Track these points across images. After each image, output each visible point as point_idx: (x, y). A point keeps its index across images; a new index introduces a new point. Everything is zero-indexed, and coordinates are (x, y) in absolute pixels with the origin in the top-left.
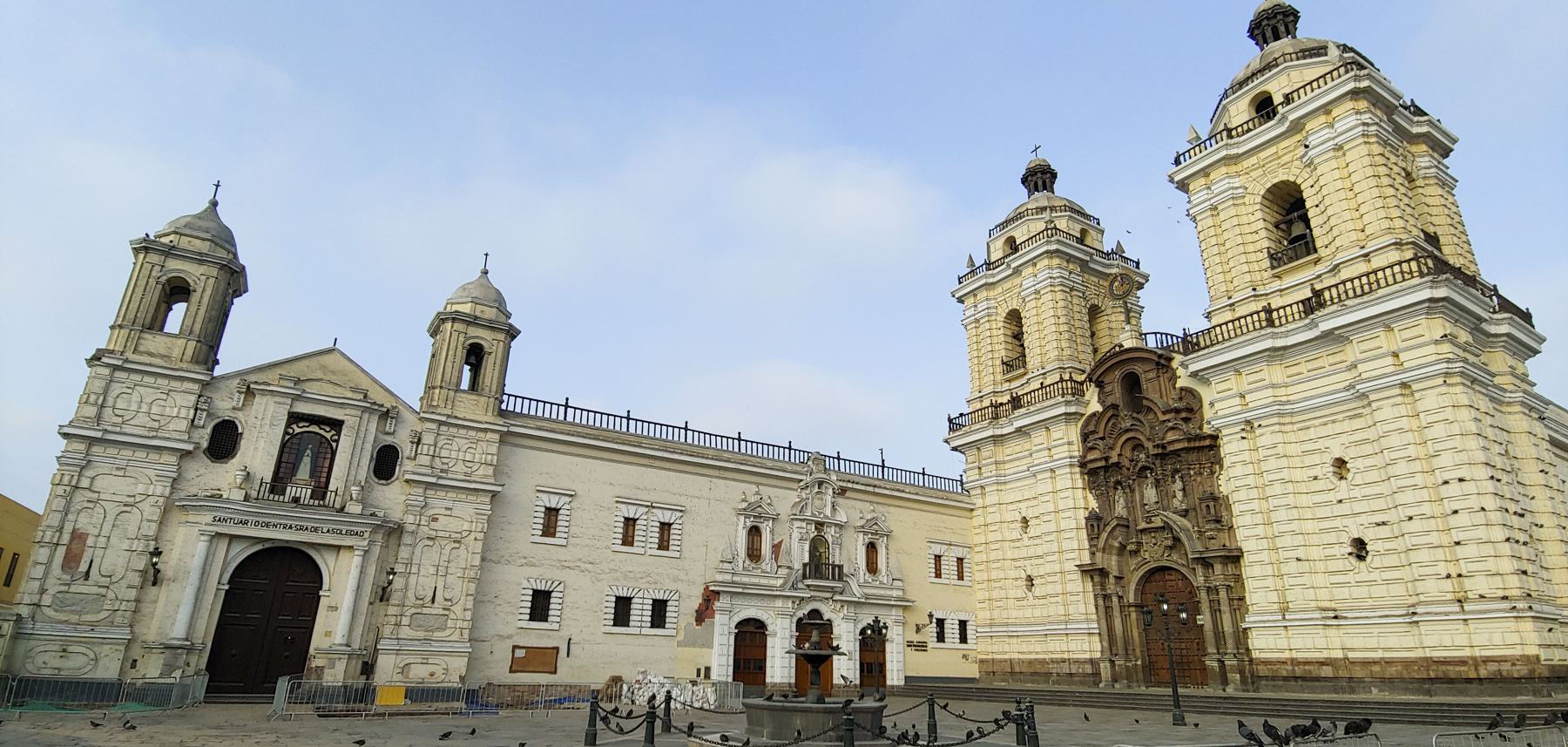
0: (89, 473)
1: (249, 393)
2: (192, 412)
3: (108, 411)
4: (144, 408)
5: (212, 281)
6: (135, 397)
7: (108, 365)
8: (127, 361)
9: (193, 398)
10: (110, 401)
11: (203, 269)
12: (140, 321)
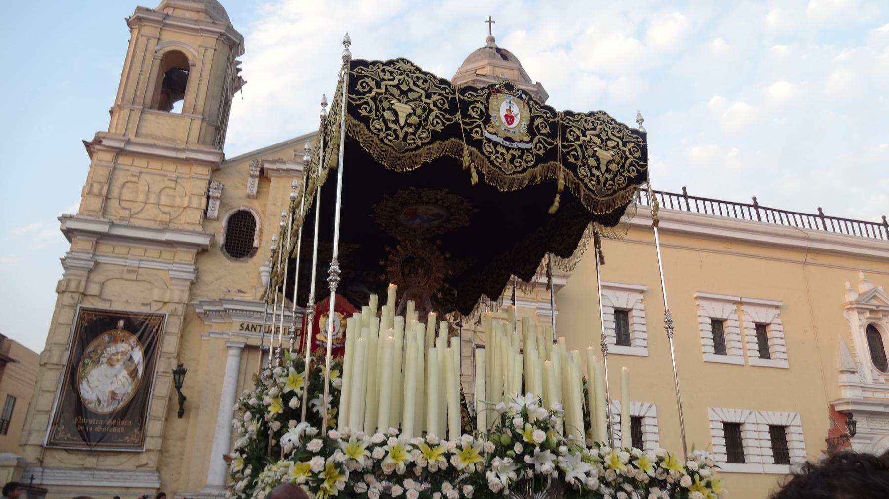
0: (98, 277)
1: (263, 176)
2: (204, 200)
3: (114, 203)
4: (153, 199)
5: (211, 52)
6: (142, 186)
7: (111, 149)
8: (129, 142)
9: (204, 185)
10: (115, 192)
11: (199, 41)
12: (140, 99)
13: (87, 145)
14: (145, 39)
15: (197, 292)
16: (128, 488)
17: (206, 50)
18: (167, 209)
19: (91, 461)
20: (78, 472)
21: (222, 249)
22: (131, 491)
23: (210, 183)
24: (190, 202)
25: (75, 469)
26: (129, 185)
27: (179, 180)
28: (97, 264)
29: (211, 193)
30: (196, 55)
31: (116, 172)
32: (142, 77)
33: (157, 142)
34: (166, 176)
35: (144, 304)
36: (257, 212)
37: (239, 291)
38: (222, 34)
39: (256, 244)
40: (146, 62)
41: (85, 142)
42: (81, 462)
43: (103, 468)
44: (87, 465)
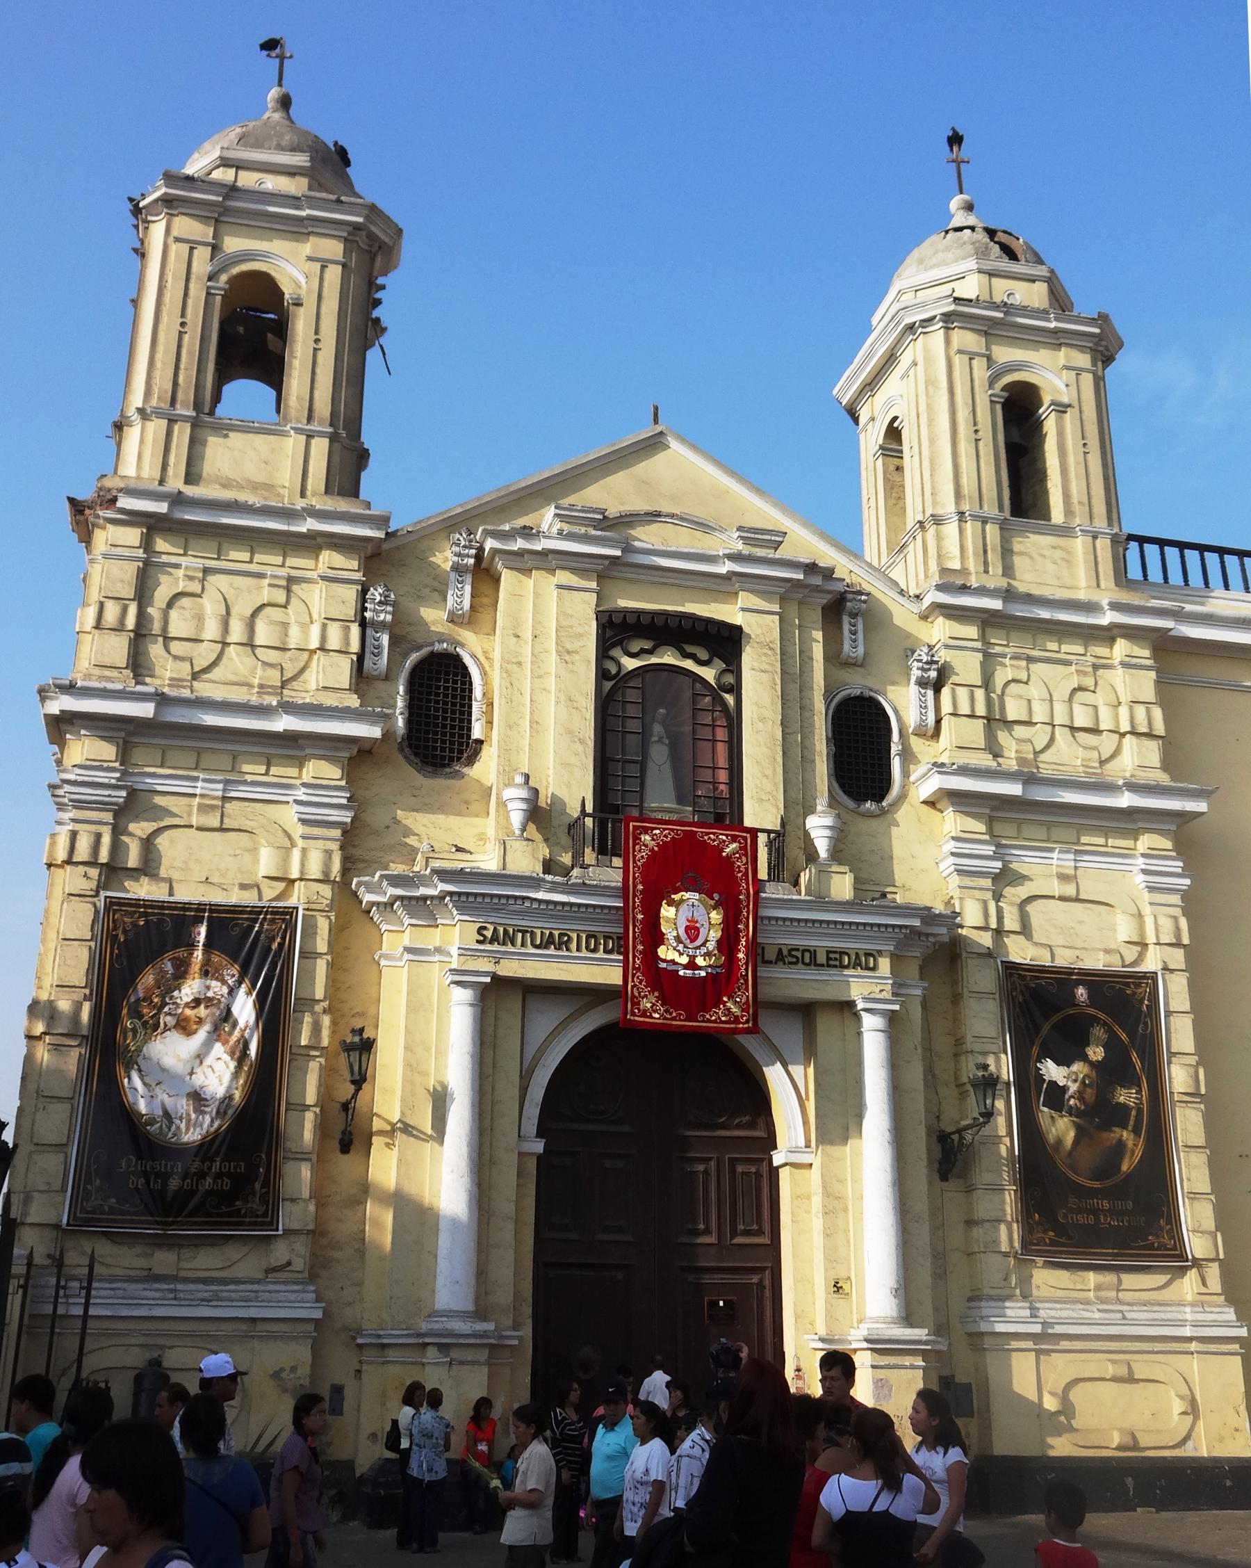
2: (355, 630)
3: (155, 650)
4: (237, 632)
5: (334, 274)
6: (211, 606)
7: (135, 518)
9: (351, 593)
13: (77, 507)
14: (185, 248)
15: (357, 852)
16: (254, 1320)
17: (323, 267)
18: (272, 656)
19: (164, 1260)
20: (140, 1286)
21: (401, 750)
22: (260, 1326)
23: (364, 591)
24: (323, 638)
25: (131, 1280)
26: (185, 602)
27: (295, 588)
28: (133, 793)
29: (368, 615)
30: (303, 281)
31: (151, 570)
32: (186, 338)
33: (242, 497)
34: (261, 576)
35: (243, 887)
36: (473, 656)
37: (459, 849)
38: (356, 227)
39: (477, 732)
40: (190, 302)
41: (72, 501)
42: (142, 1263)
43: (190, 1274)
44: (157, 1270)
